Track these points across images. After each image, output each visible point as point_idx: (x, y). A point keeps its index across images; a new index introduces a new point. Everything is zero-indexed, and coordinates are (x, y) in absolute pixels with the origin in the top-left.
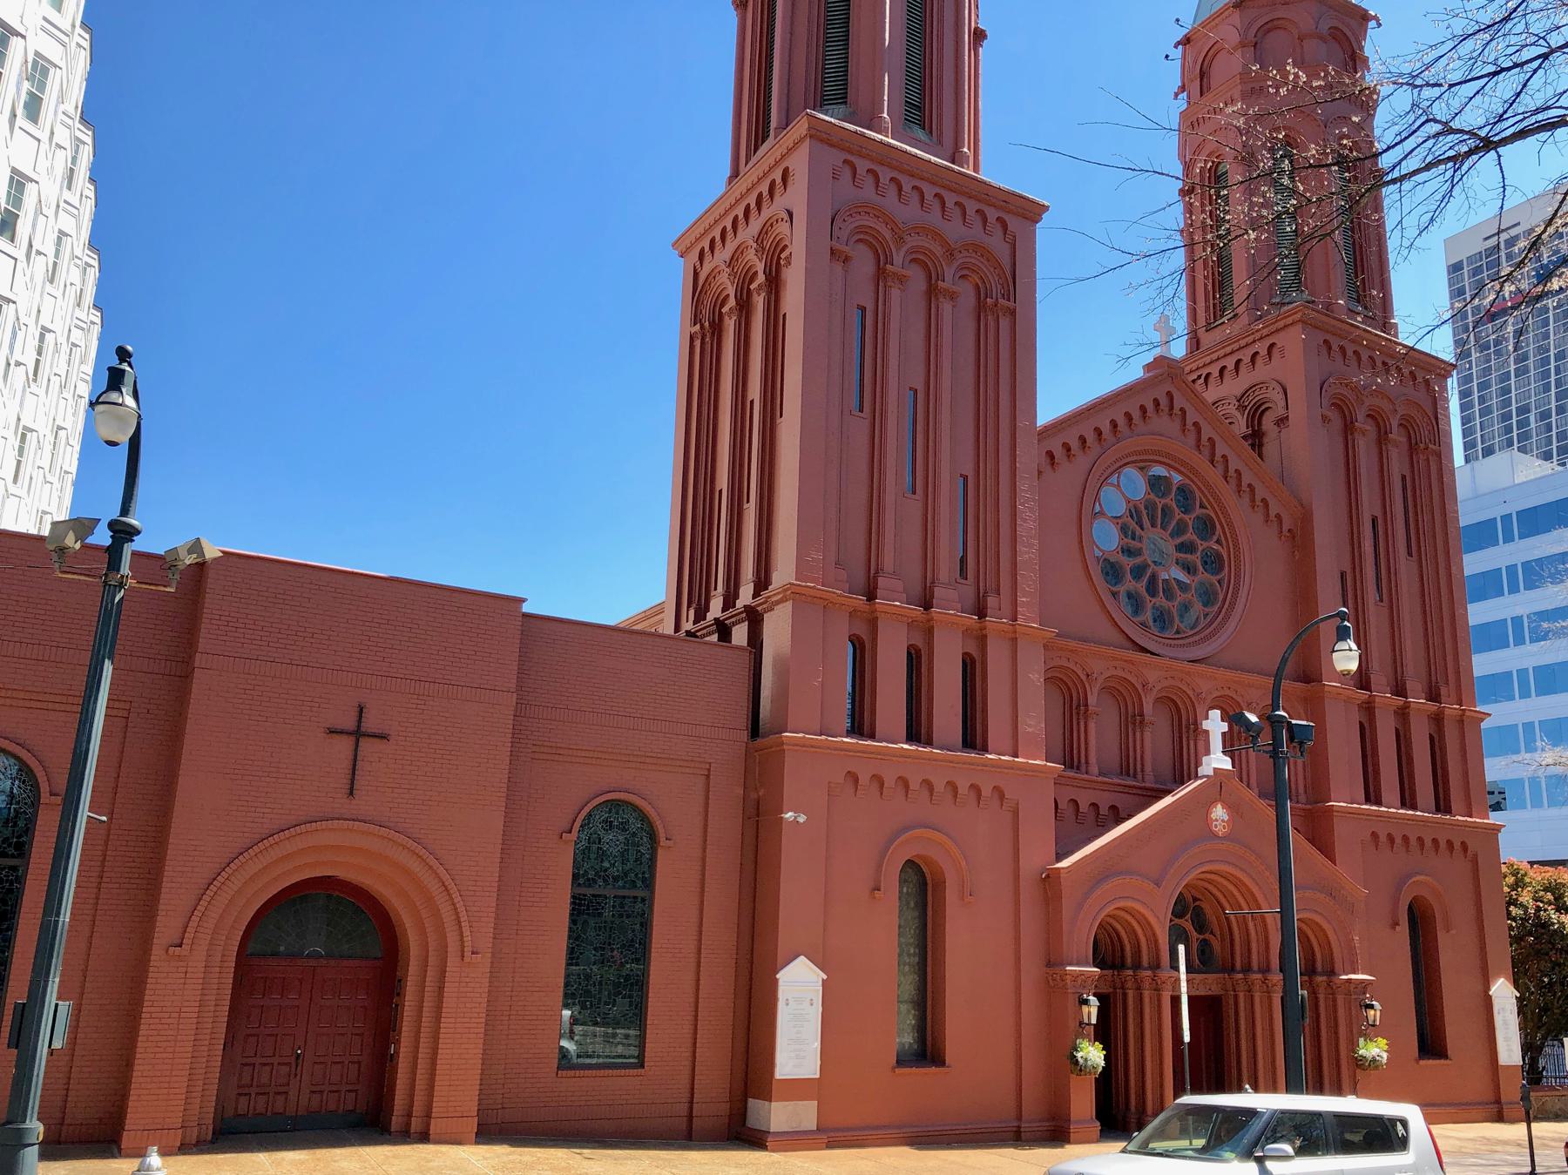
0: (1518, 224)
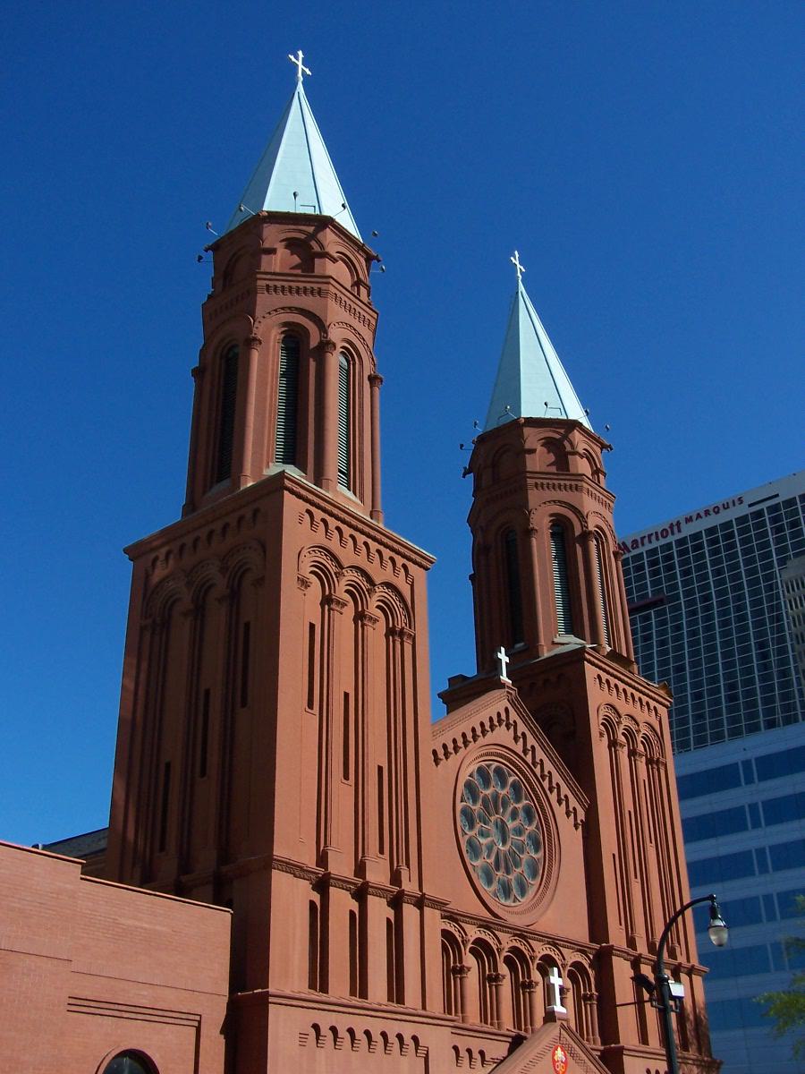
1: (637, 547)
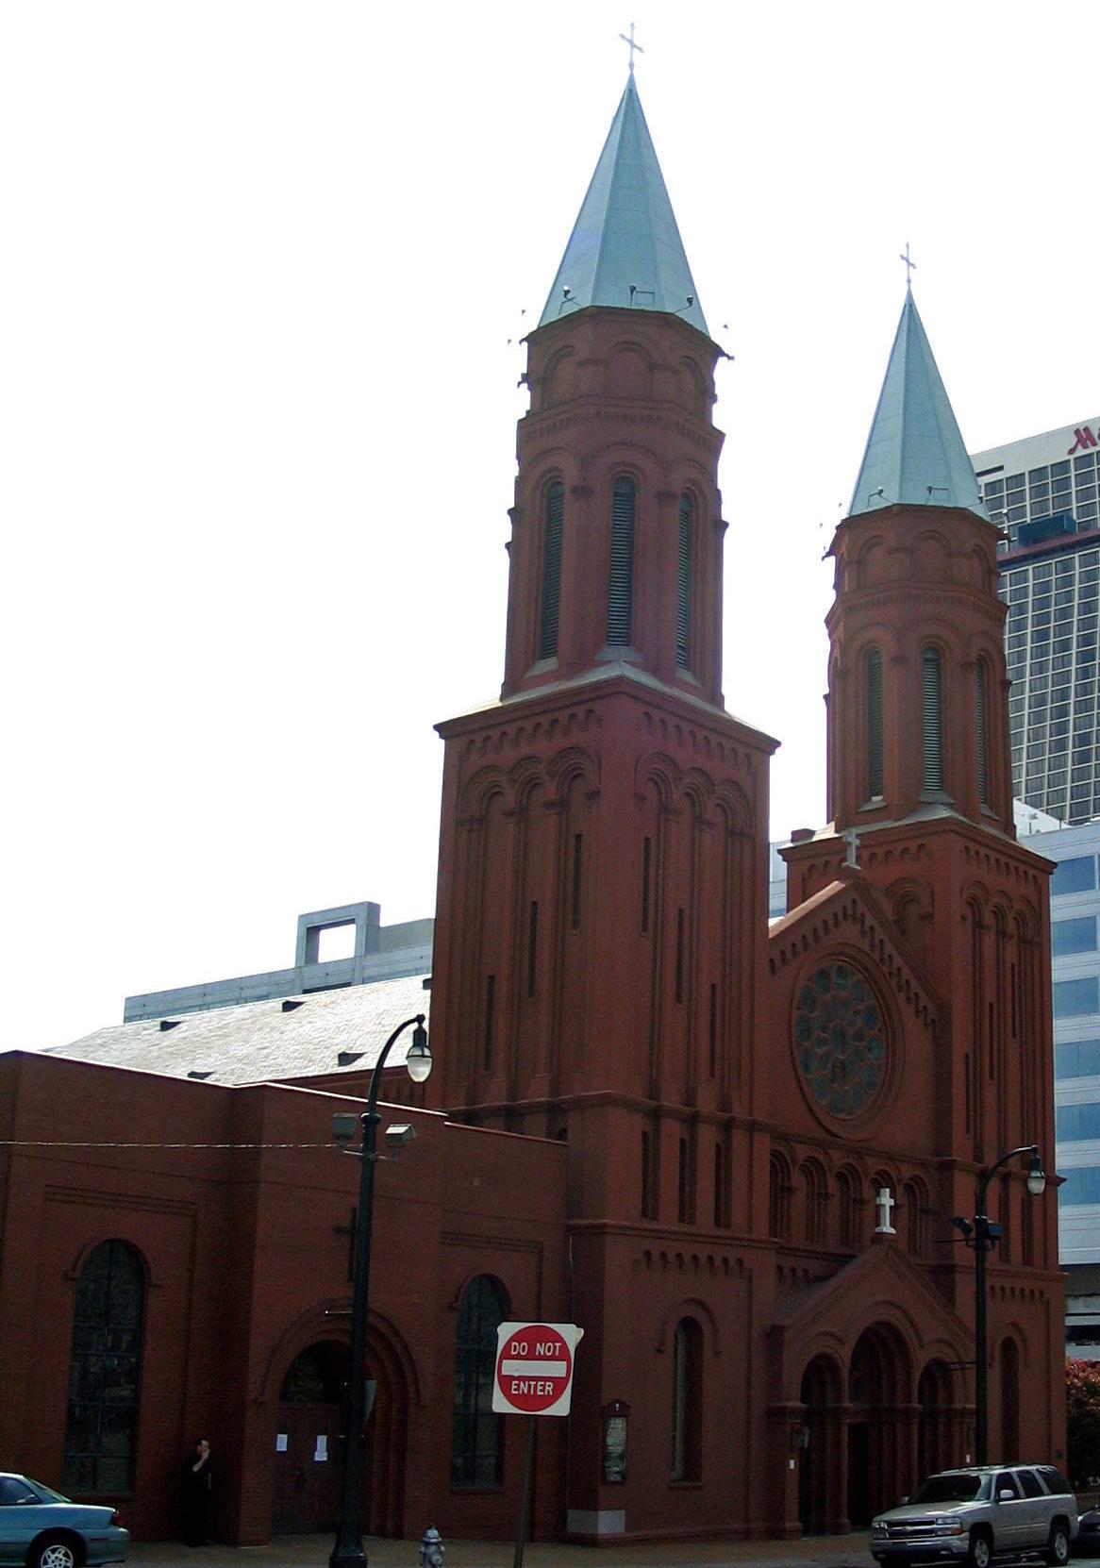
0: (1001, 468)
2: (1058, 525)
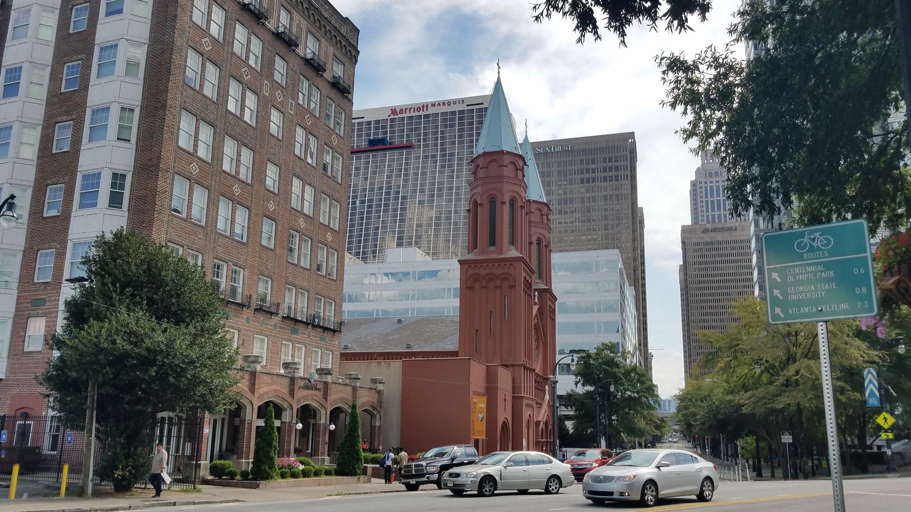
1: (402, 113)
2: (383, 141)
